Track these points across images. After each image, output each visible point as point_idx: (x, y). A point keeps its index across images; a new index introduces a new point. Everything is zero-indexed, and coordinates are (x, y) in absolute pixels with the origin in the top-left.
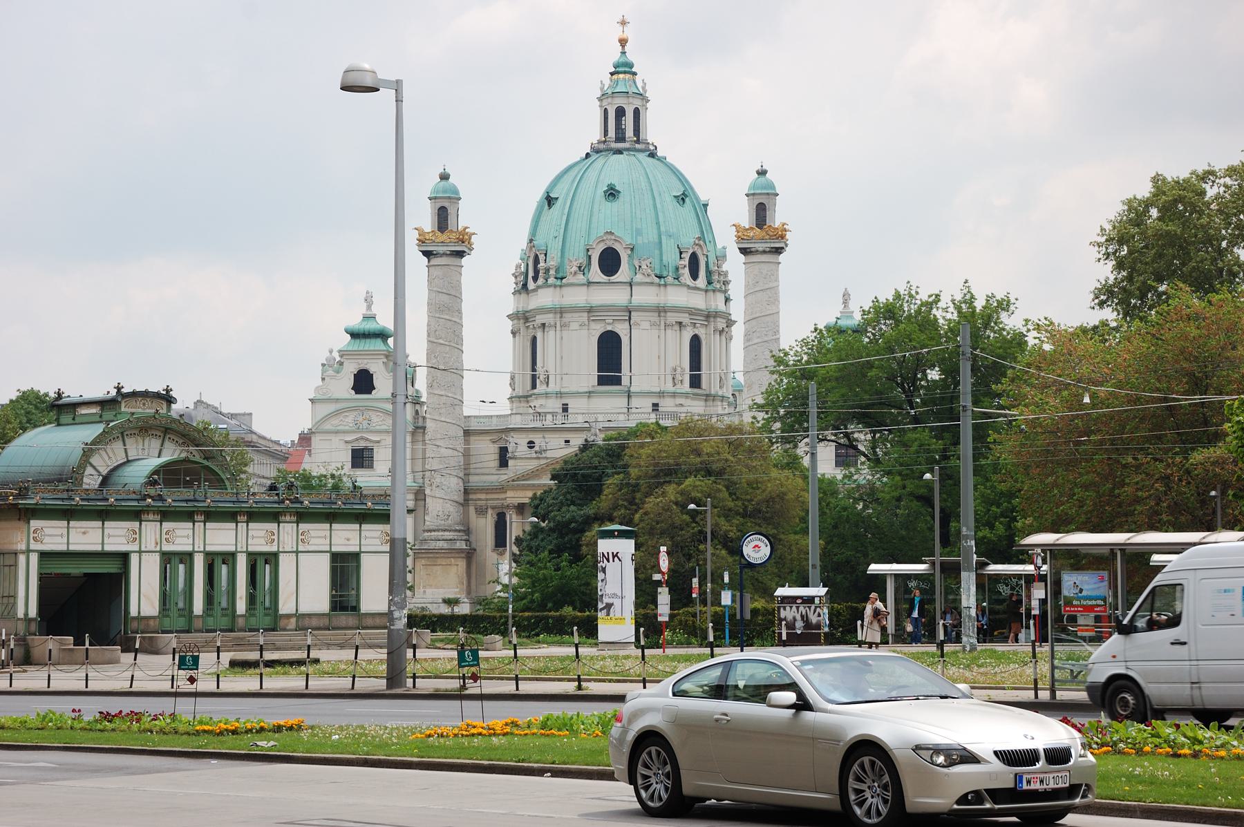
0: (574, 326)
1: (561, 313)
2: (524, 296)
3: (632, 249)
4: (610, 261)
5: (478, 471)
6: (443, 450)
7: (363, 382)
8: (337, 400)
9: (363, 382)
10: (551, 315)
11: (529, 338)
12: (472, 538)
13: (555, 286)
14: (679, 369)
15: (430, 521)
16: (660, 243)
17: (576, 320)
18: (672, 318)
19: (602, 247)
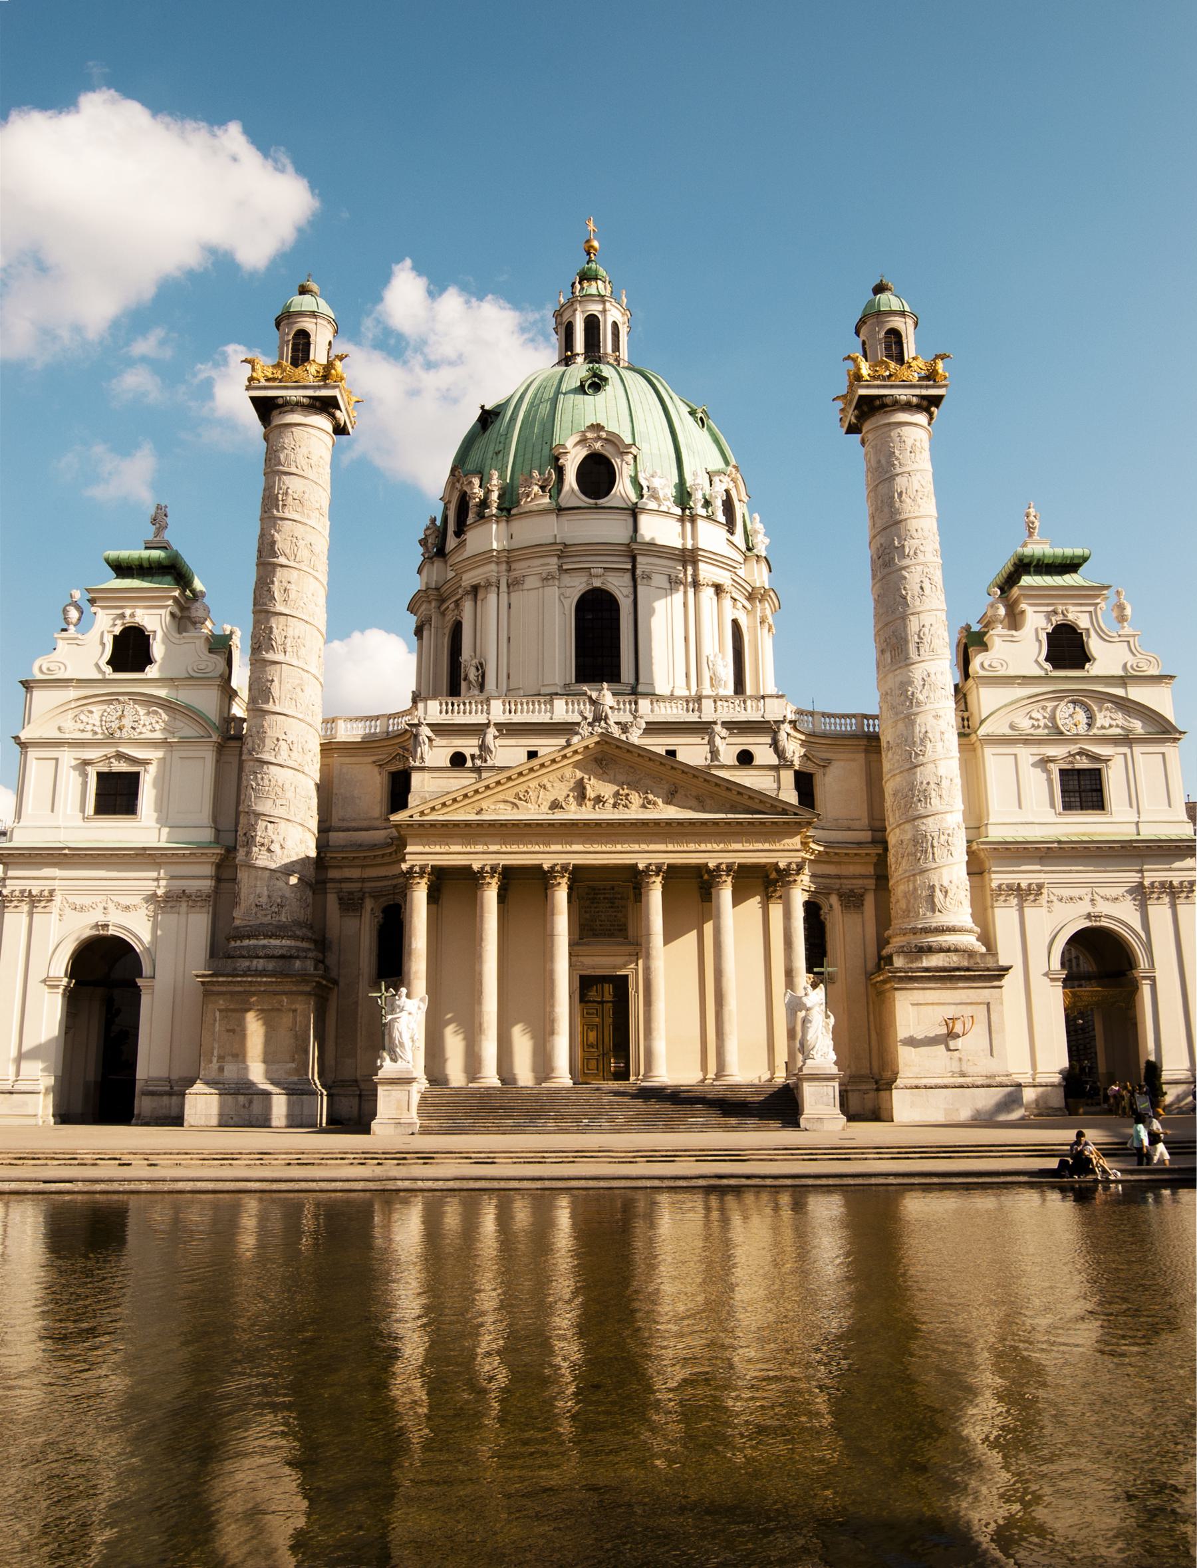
0: (532, 582)
2: (438, 564)
3: (635, 457)
4: (598, 474)
5: (345, 824)
10: (493, 567)
11: (447, 631)
12: (331, 960)
14: (719, 662)
15: (240, 917)
17: (532, 570)
19: (582, 453)
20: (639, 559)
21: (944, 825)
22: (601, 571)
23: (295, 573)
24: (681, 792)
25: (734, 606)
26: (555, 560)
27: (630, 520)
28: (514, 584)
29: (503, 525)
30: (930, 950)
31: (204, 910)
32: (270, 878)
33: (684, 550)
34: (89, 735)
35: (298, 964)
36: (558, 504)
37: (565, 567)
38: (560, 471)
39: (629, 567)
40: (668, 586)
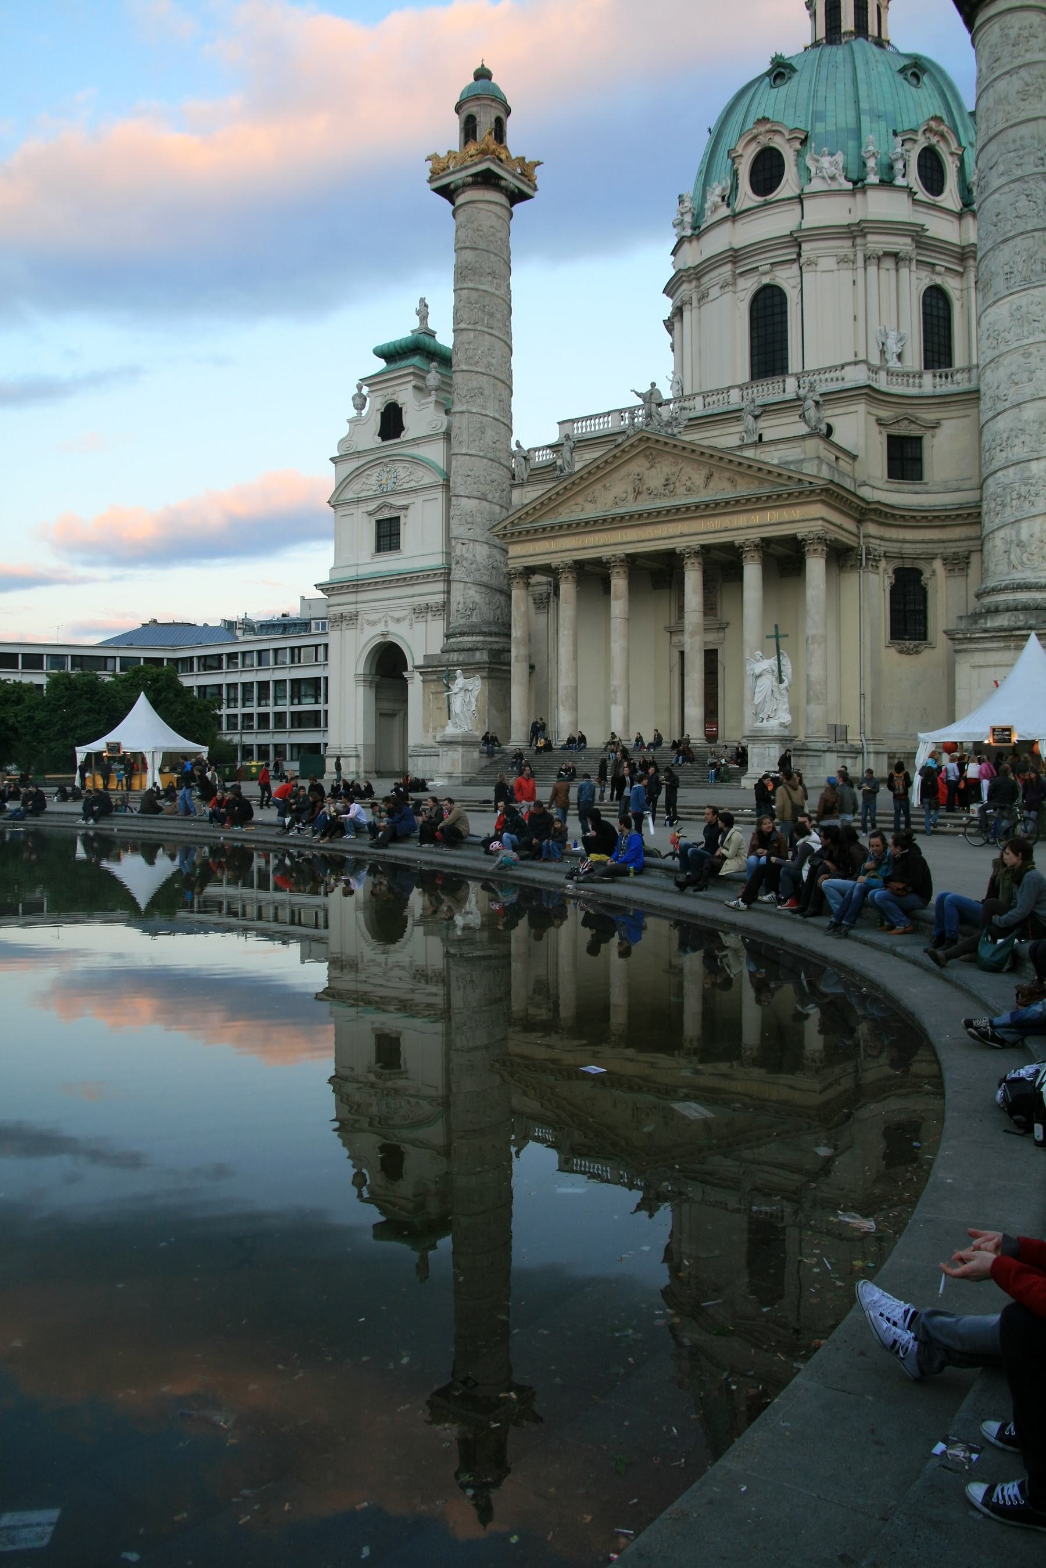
0: (714, 292)
1: (698, 279)
3: (804, 142)
4: (767, 171)
6: (464, 500)
7: (391, 422)
8: (359, 454)
9: (391, 422)
10: (685, 286)
13: (690, 239)
14: (893, 335)
16: (859, 129)
18: (877, 243)
19: (753, 150)
20: (805, 246)
21: (1027, 474)
22: (768, 267)
23: (472, 334)
24: (716, 475)
25: (933, 272)
26: (729, 267)
27: (798, 207)
28: (703, 297)
29: (695, 242)
30: (994, 611)
31: (441, 617)
32: (465, 588)
33: (848, 226)
34: (371, 493)
35: (478, 654)
36: (733, 210)
37: (738, 271)
38: (735, 174)
39: (794, 256)
40: (835, 267)
